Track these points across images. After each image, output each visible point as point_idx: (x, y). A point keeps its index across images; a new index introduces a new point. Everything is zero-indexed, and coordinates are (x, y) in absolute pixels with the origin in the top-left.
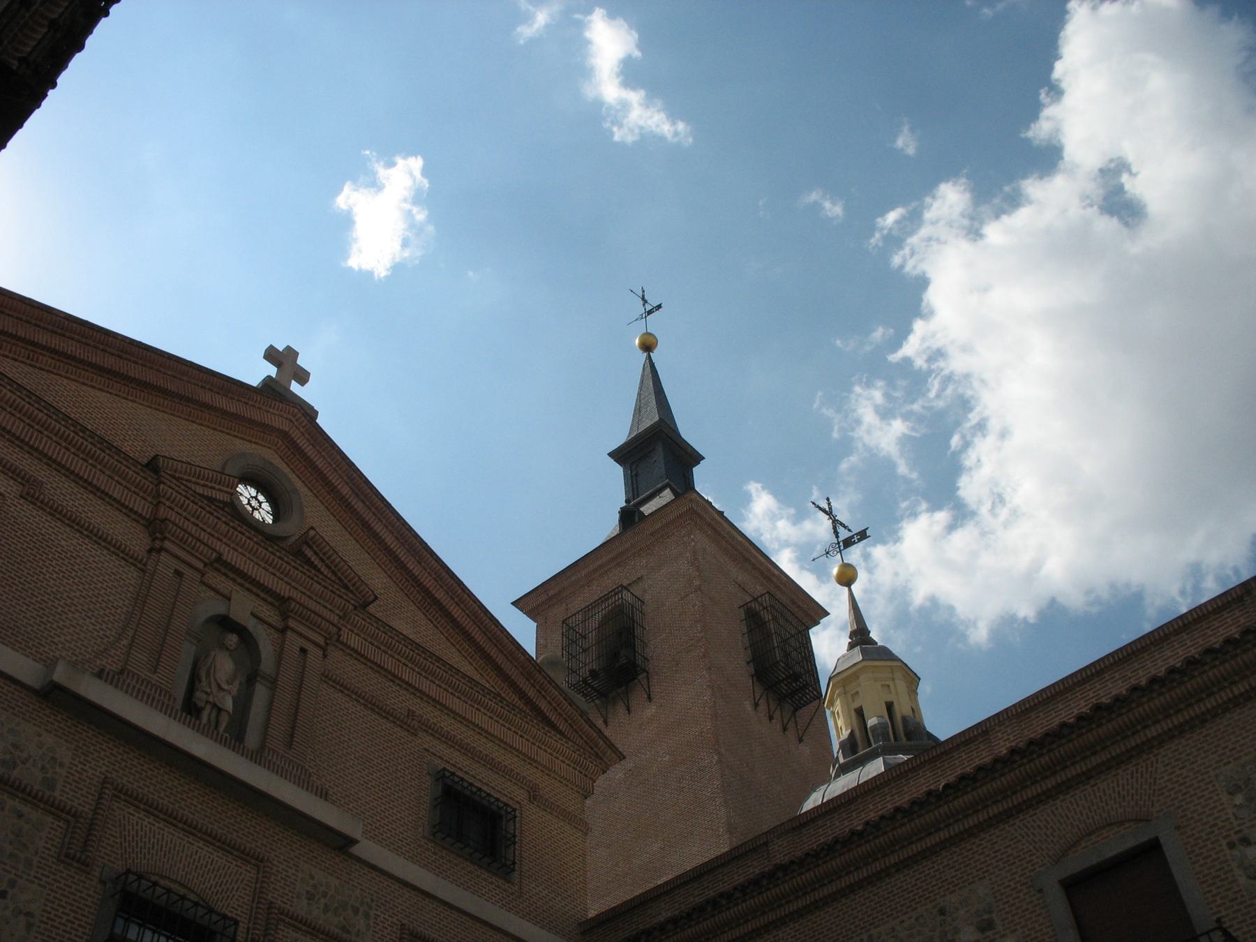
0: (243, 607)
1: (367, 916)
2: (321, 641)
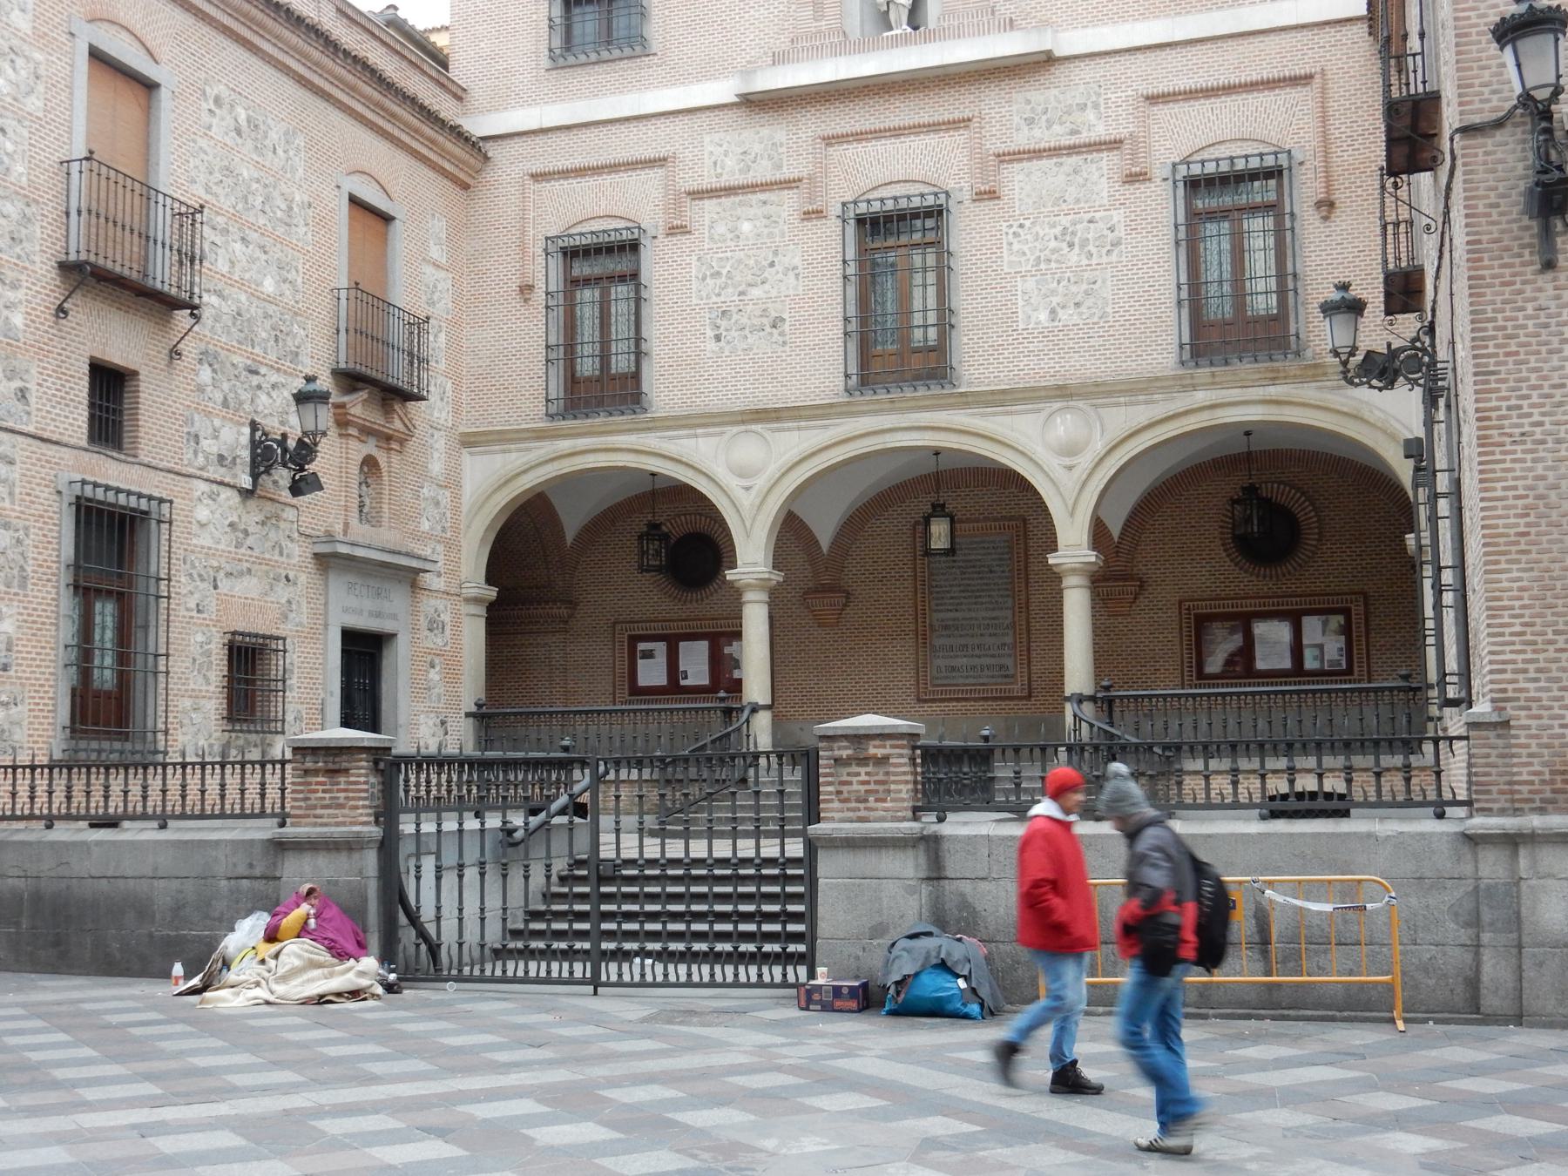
1: (1096, 106)
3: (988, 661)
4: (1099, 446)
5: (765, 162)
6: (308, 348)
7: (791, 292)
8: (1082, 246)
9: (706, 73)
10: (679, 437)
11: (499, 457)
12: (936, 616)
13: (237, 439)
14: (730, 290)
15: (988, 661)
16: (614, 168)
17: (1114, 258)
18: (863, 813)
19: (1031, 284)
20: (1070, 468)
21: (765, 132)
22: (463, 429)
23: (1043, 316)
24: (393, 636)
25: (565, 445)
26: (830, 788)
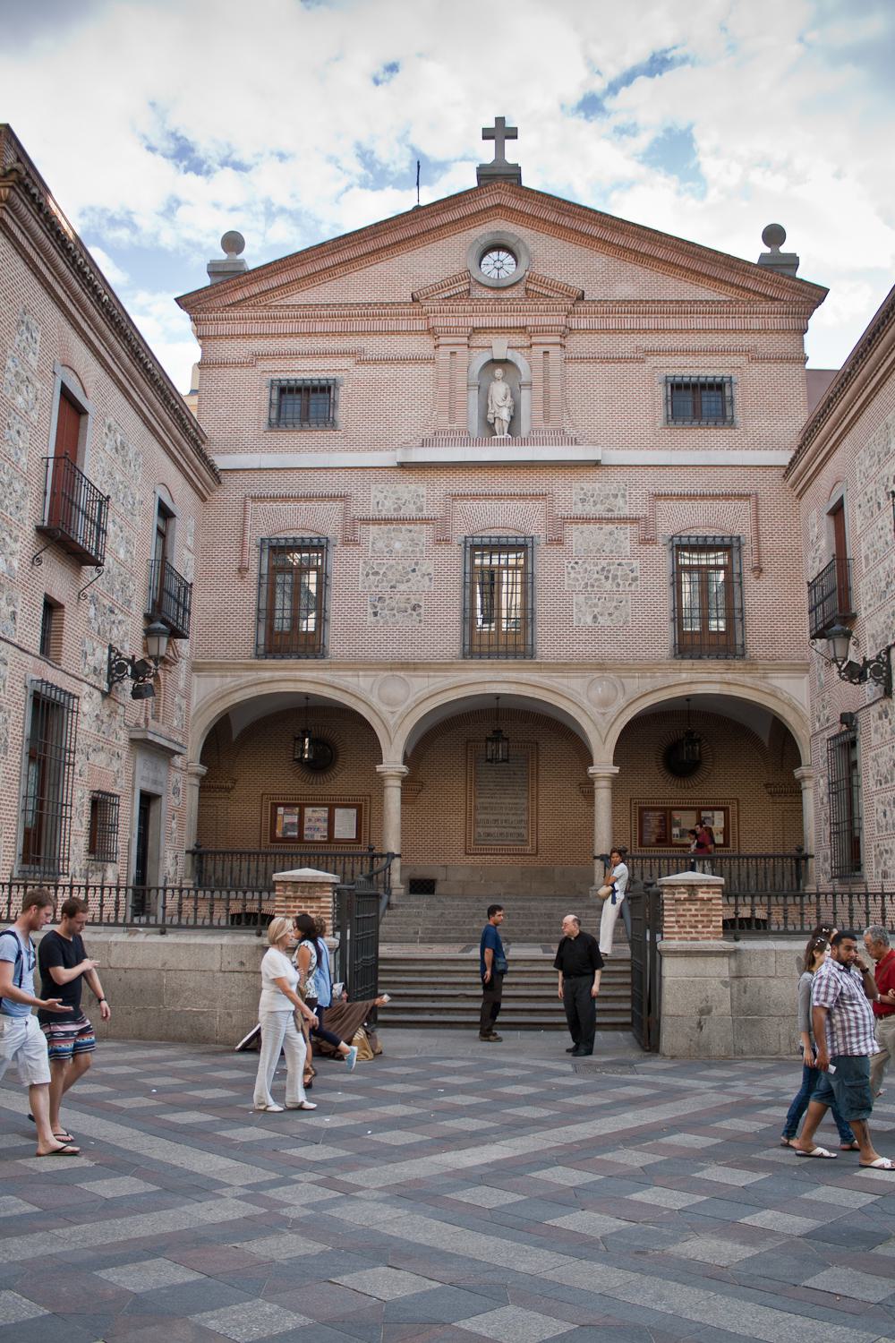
0: (500, 347)
1: (624, 496)
2: (558, 339)
3: (512, 830)
4: (622, 702)
5: (412, 506)
6: (135, 599)
7: (426, 589)
8: (614, 579)
9: (374, 446)
10: (346, 676)
11: (218, 680)
13: (100, 657)
14: (384, 584)
15: (512, 830)
16: (309, 498)
17: (633, 588)
18: (694, 935)
19: (581, 598)
20: (604, 714)
21: (413, 487)
22: (193, 659)
23: (589, 620)
24: (160, 796)
25: (267, 675)
26: (673, 919)
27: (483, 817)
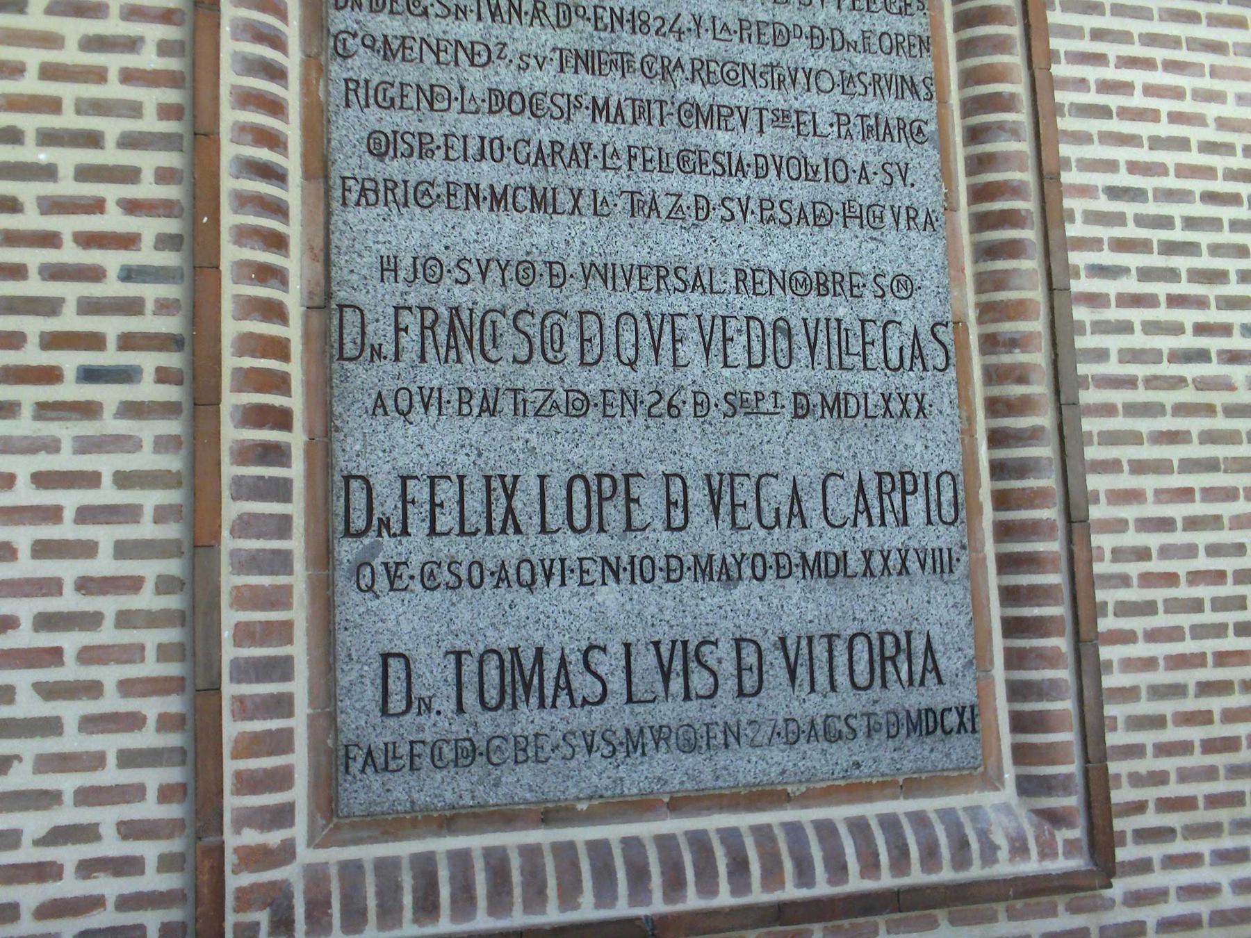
3: (797, 606)
12: (373, 231)
15: (797, 606)
27: (433, 442)
